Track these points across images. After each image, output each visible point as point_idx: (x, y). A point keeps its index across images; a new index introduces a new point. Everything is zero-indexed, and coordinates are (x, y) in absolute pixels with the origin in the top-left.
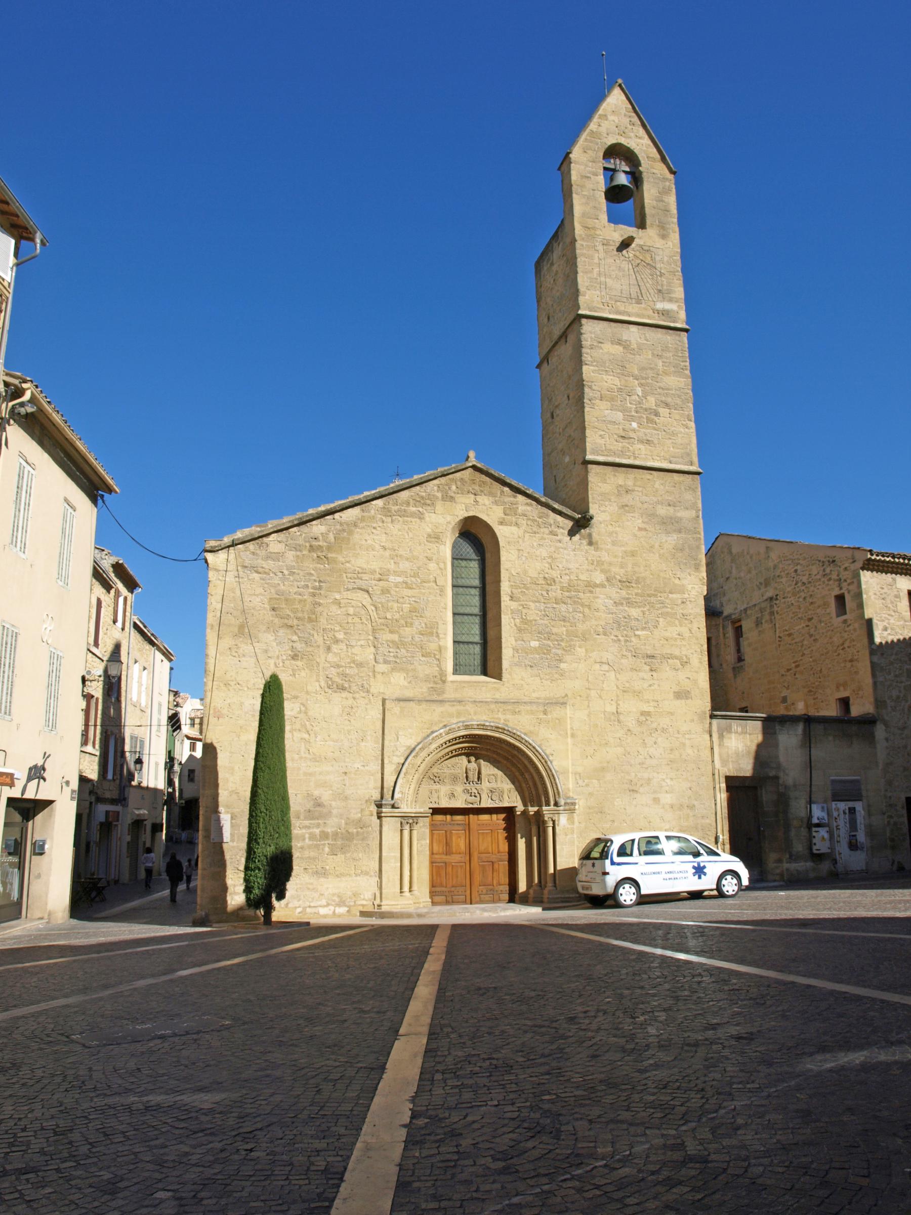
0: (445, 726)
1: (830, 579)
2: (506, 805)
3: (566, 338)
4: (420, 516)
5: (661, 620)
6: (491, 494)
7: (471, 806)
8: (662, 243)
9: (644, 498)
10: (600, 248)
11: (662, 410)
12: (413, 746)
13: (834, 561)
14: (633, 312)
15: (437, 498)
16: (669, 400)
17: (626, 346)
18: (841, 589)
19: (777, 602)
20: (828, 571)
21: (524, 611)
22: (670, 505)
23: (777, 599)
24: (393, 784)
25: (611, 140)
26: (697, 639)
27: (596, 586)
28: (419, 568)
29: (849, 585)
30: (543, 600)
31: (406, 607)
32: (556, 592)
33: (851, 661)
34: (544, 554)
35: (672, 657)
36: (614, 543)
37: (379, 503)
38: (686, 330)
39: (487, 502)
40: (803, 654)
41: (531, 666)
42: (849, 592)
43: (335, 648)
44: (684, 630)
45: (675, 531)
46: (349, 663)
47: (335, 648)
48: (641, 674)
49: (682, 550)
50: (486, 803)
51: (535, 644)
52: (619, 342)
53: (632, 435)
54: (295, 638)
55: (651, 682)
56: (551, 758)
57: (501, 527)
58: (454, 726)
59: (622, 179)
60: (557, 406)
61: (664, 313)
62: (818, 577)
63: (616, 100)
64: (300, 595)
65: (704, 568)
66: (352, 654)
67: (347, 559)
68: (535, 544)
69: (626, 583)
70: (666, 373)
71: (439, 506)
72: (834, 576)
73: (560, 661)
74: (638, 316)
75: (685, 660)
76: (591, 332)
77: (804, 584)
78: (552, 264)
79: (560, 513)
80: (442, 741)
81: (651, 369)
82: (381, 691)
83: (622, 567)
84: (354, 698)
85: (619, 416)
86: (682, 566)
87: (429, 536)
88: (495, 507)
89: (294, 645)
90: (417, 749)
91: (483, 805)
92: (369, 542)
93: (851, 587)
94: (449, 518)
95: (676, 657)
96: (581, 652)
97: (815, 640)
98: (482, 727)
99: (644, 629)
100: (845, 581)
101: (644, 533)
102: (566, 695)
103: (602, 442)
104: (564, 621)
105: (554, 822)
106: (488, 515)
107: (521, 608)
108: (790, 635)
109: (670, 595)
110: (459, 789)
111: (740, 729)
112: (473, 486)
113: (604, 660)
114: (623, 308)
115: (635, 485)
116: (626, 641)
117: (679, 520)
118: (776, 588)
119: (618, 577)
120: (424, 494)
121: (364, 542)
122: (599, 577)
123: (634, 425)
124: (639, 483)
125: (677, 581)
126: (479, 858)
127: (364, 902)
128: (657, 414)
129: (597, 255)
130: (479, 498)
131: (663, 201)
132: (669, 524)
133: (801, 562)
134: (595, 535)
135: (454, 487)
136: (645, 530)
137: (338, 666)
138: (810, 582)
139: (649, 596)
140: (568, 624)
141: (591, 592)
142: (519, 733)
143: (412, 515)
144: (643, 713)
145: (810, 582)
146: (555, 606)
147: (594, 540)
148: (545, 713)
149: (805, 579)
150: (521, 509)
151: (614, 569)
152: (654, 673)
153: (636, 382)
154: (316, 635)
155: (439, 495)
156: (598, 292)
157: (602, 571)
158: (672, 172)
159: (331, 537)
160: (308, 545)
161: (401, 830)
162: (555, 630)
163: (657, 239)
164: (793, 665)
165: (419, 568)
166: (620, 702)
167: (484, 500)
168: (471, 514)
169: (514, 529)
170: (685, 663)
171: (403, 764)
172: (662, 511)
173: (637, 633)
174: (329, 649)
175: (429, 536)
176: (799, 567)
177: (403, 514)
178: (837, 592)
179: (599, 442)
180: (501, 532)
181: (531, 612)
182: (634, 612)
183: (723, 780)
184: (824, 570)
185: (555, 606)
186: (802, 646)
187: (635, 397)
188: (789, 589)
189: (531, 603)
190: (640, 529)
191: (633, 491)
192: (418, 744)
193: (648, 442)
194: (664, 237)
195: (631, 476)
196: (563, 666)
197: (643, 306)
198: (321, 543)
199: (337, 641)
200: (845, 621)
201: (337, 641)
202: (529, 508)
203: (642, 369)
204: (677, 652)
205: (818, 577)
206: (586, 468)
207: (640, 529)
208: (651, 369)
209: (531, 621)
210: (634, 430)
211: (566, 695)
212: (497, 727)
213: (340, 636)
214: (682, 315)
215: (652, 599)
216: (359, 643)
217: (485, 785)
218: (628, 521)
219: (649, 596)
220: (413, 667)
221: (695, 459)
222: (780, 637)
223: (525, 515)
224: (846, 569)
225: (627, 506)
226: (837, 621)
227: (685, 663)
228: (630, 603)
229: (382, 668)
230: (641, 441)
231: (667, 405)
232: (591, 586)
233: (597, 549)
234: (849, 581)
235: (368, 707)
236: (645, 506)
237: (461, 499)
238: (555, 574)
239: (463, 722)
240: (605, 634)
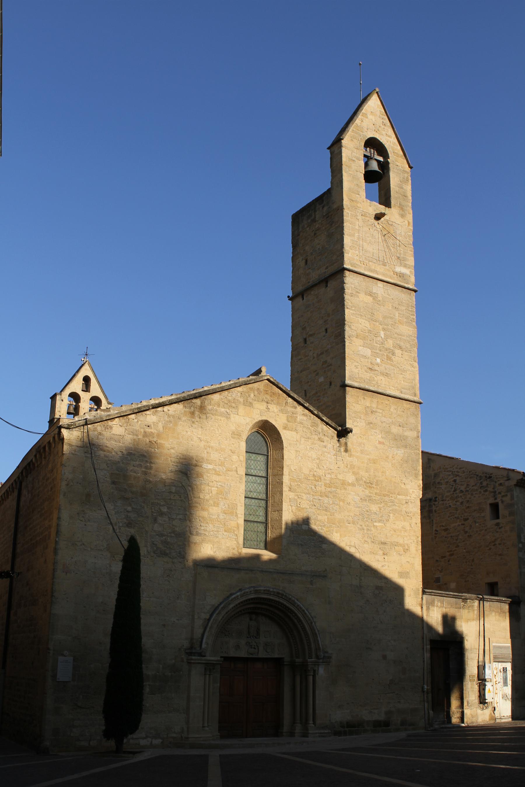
0: (240, 590)
1: (486, 491)
2: (276, 656)
3: (327, 282)
4: (227, 416)
5: (391, 515)
6: (278, 404)
7: (251, 656)
8: (401, 219)
9: (384, 419)
10: (360, 217)
12: (216, 605)
13: (490, 477)
14: (380, 272)
15: (240, 403)
16: (402, 344)
18: (496, 499)
19: (436, 503)
20: (485, 484)
21: (299, 500)
22: (400, 426)
23: (436, 501)
24: (200, 636)
25: (370, 135)
26: (415, 532)
27: (349, 484)
28: (225, 458)
29: (503, 496)
30: (312, 493)
32: (321, 488)
33: (500, 555)
34: (314, 456)
35: (397, 544)
36: (362, 452)
38: (415, 291)
39: (276, 410)
40: (458, 546)
41: (302, 545)
42: (502, 502)
43: (160, 520)
44: (406, 524)
45: (403, 446)
46: (170, 533)
47: (160, 520)
48: (377, 557)
49: (407, 462)
50: (262, 654)
52: (370, 294)
53: (376, 368)
54: (129, 509)
55: (383, 564)
57: (285, 431)
58: (247, 590)
59: (374, 166)
60: (311, 335)
61: (401, 275)
62: (475, 488)
63: (374, 104)
64: (135, 472)
65: (421, 477)
66: (173, 525)
67: (172, 446)
68: (308, 447)
69: (369, 484)
70: (400, 322)
71: (241, 409)
72: (490, 489)
74: (383, 275)
75: (407, 547)
76: (352, 284)
77: (462, 491)
78: (314, 221)
79: (327, 424)
80: (237, 602)
81: (391, 318)
83: (367, 472)
84: (173, 563)
85: (368, 352)
86: (406, 474)
87: (233, 433)
88: (281, 414)
89: (129, 514)
91: (260, 656)
92: (189, 433)
93: (504, 499)
94: (248, 420)
95: (400, 545)
97: (470, 536)
98: (268, 592)
99: (380, 521)
100: (500, 493)
101: (382, 446)
102: (326, 570)
103: (356, 371)
104: (326, 510)
105: (314, 671)
106: (276, 420)
107: (296, 498)
108: (446, 530)
109: (398, 497)
111: (439, 604)
112: (266, 396)
113: (352, 544)
114: (373, 268)
115: (377, 408)
116: (368, 530)
117: (405, 438)
118: (435, 492)
119: (364, 479)
120: (230, 398)
121: (185, 433)
122: (350, 478)
123: (378, 360)
124: (380, 407)
125: (403, 486)
127: (174, 735)
128: (393, 354)
129: (357, 223)
130: (270, 406)
131: (402, 188)
132: (399, 440)
133: (460, 474)
134: (349, 444)
135: (252, 395)
136: (383, 443)
137: (162, 535)
138: (467, 491)
139: (384, 495)
140: (329, 513)
141: (345, 489)
142: (293, 599)
143: (222, 414)
145: (467, 491)
146: (320, 498)
147: (348, 448)
148: (311, 583)
149: (463, 488)
150: (300, 418)
151: (362, 473)
152: (386, 557)
153: (381, 327)
154: (146, 508)
155: (241, 400)
156: (357, 252)
157: (354, 473)
158: (411, 167)
159: (160, 426)
160: (142, 430)
162: (320, 517)
163: (397, 216)
164: (448, 554)
165: (225, 458)
166: (363, 578)
167: (274, 408)
168: (264, 418)
169: (294, 433)
170: (406, 550)
171: (209, 620)
172: (395, 430)
173: (375, 524)
174: (155, 520)
175: (233, 433)
176: (457, 478)
178: (491, 500)
179: (354, 371)
180: (285, 435)
181: (303, 502)
182: (374, 508)
183: (428, 642)
184: (481, 483)
185: (320, 498)
186: (457, 540)
187: (379, 339)
188: (448, 494)
189: (304, 495)
190: (380, 443)
191: (376, 412)
192: (221, 604)
193: (387, 375)
194: (402, 216)
195: (375, 401)
197: (387, 267)
198: (152, 430)
199: (162, 514)
200: (497, 524)
201: (162, 514)
202: (305, 418)
203: (385, 317)
204: (401, 541)
205: (475, 488)
206: (345, 390)
207: (380, 443)
208: (391, 318)
209: (303, 509)
210: (378, 364)
211: (326, 570)
212: (278, 593)
213: (165, 509)
214: (413, 279)
215: (386, 499)
216: (179, 517)
218: (372, 435)
219: (384, 495)
220: (217, 540)
221: (418, 392)
222: (436, 530)
223: (302, 423)
224: (501, 484)
225: (371, 423)
226: (491, 523)
227: (406, 550)
228: (370, 499)
230: (382, 374)
231: (400, 348)
232: (344, 484)
233: (350, 456)
234: (503, 494)
236: (384, 425)
237: (257, 405)
238: (320, 472)
239: (254, 587)
240: (354, 523)
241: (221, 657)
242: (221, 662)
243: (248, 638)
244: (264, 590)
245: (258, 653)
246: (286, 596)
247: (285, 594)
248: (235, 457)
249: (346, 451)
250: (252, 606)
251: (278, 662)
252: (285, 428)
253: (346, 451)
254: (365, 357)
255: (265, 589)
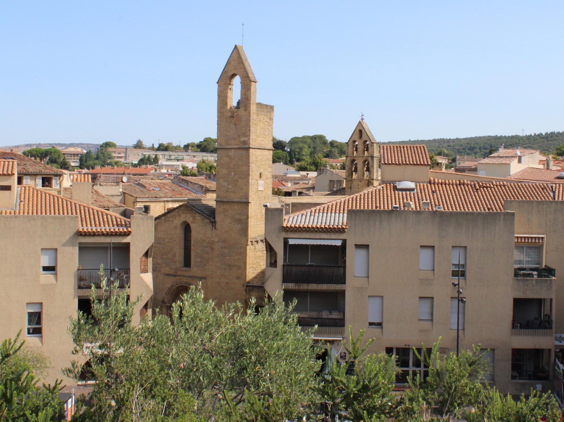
11: (240, 180)
17: (229, 157)
31: (169, 248)
35: (236, 266)
37: (163, 218)
51: (199, 260)
73: (205, 265)
85: (226, 184)
96: (211, 263)
122: (216, 240)
123: (230, 186)
144: (227, 283)
167: (188, 216)
172: (237, 217)
177: (169, 221)
180: (192, 225)
182: (226, 251)
196: (206, 267)
207: (230, 223)
228: (225, 247)
229: (164, 265)
231: (241, 178)
248: (175, 236)
249: (215, 228)
252: (192, 223)
253: (215, 228)
254: (224, 186)
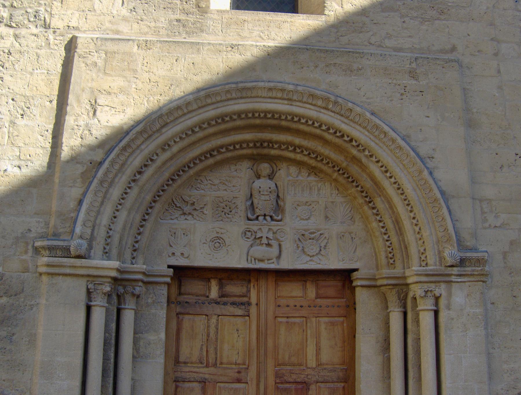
56: (430, 164)
82: (73, 24)
90: (134, 132)
91: (285, 264)
110: (234, 229)
126: (277, 375)
148: (413, 74)
161: (89, 309)
217: (291, 224)
235: (42, 52)
241: (169, 267)
242: (168, 280)
243: (249, 219)
244: (270, 89)
245: (279, 257)
246: (336, 103)
247: (333, 98)
250: (248, 136)
251: (345, 276)
255: (272, 85)
